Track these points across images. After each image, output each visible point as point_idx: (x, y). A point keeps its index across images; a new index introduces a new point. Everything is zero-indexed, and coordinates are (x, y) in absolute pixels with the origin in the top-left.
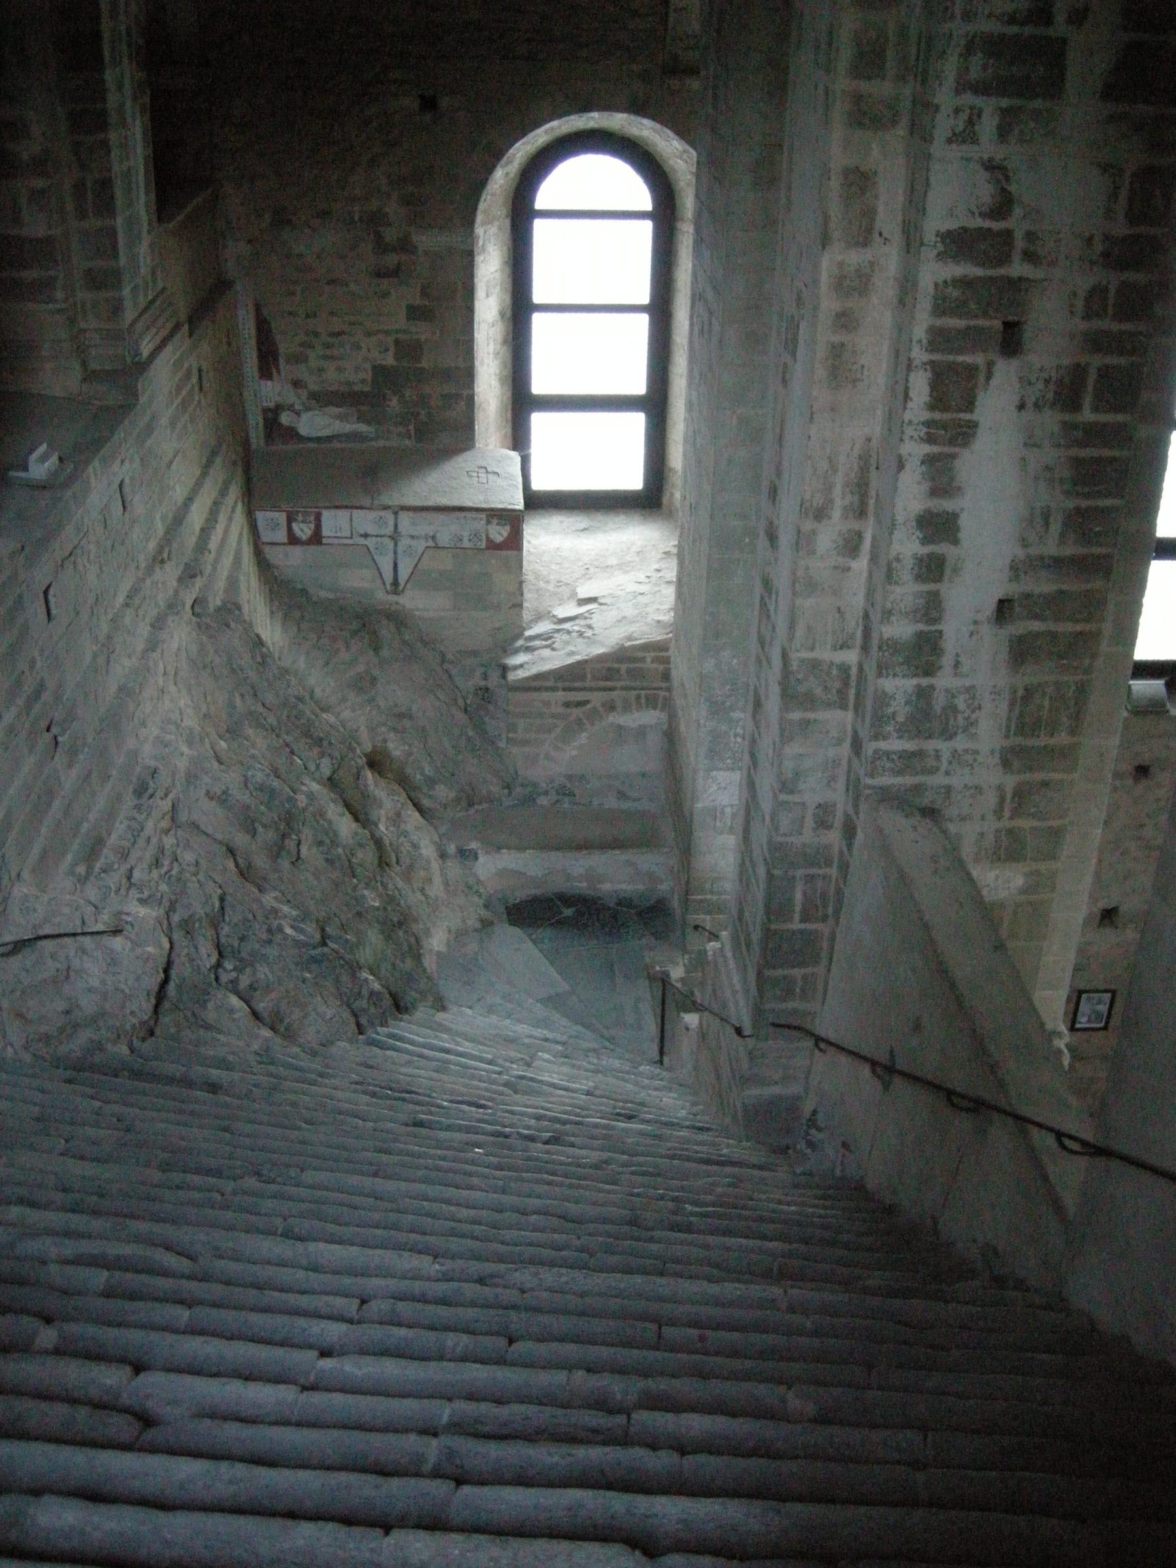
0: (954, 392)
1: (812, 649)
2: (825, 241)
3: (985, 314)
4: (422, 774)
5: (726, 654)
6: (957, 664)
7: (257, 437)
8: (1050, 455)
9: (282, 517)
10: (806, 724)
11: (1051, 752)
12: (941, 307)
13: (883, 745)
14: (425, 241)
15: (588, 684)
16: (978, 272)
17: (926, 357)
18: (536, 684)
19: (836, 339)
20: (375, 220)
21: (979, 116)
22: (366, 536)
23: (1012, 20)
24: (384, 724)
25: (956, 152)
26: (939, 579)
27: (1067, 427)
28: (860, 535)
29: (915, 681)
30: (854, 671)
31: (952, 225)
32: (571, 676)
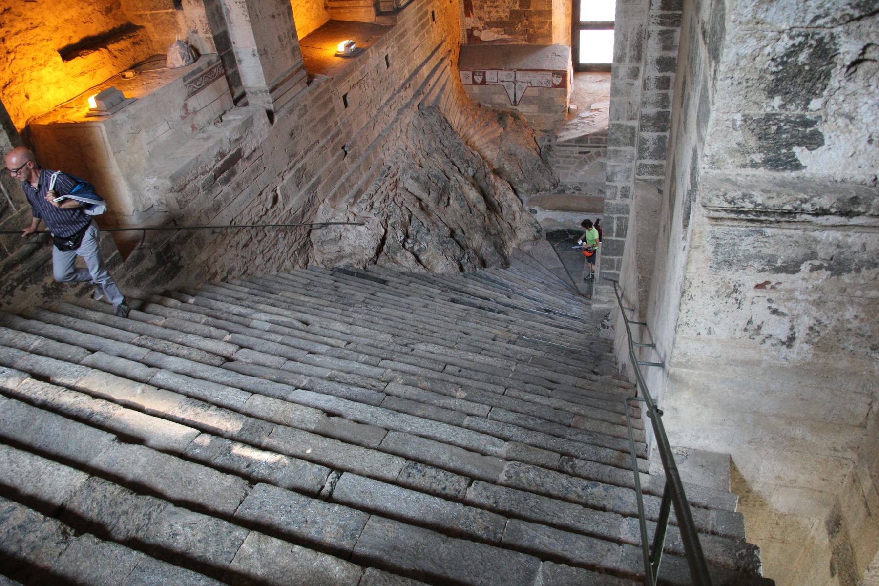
1: (618, 119)
9: (470, 74)
10: (616, 152)
15: (589, 144)
22: (503, 81)
26: (667, 88)
28: (638, 69)
32: (582, 140)
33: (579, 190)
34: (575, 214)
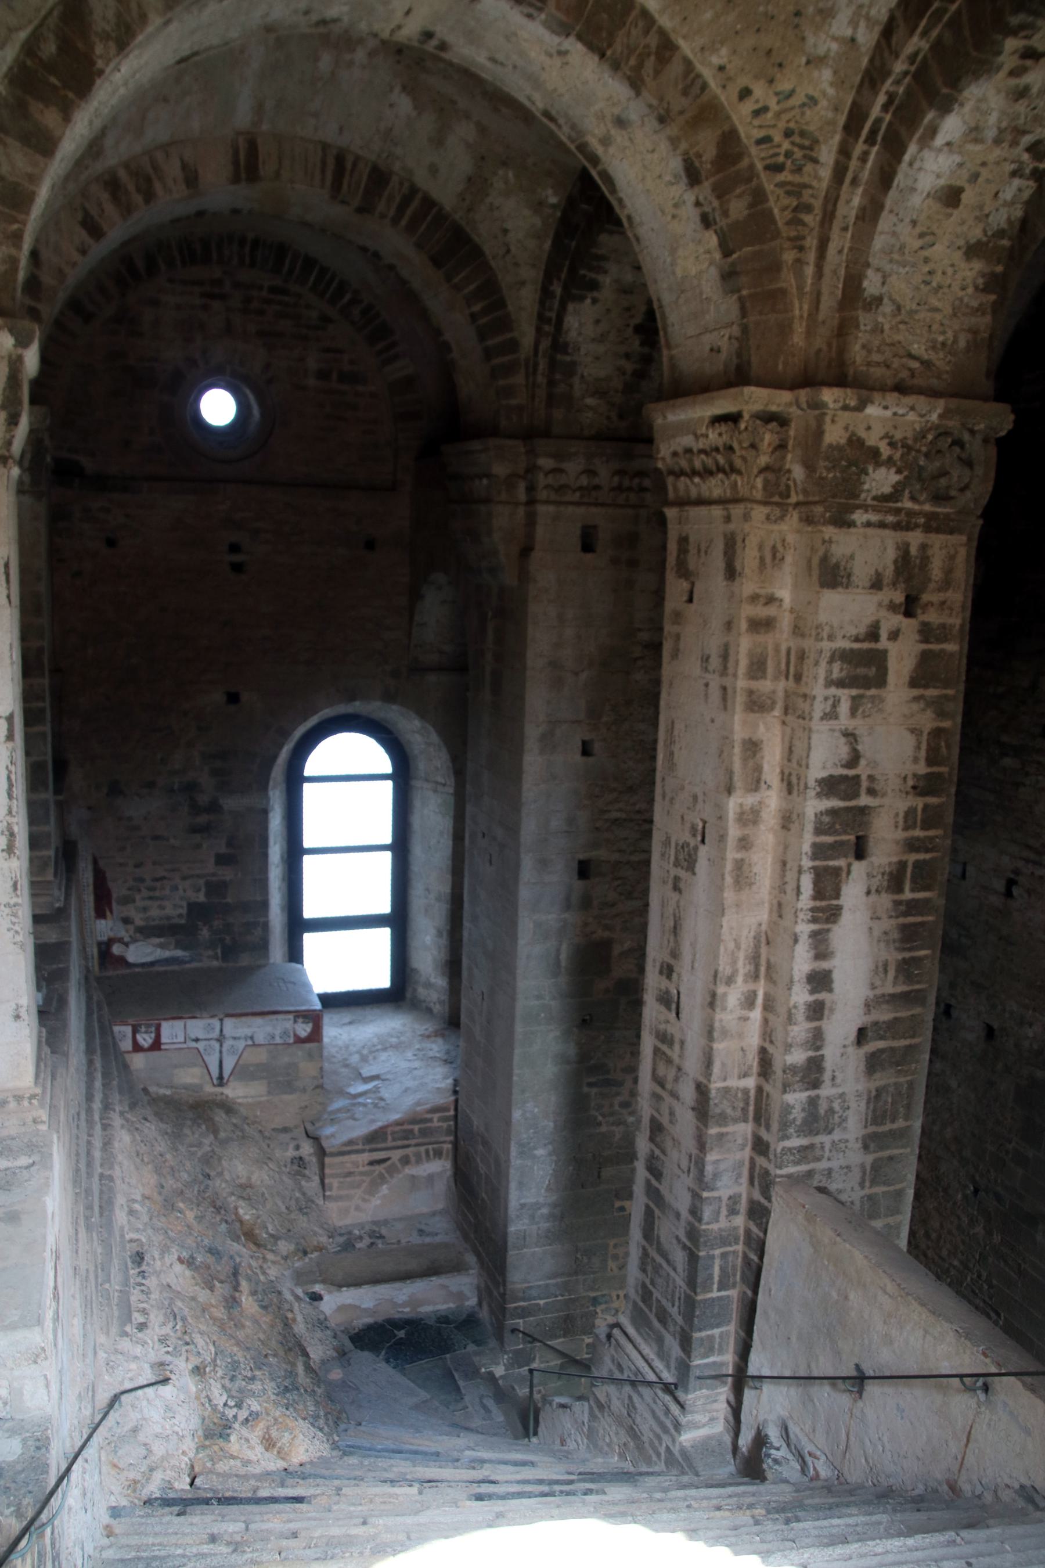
0: (828, 885)
1: (725, 1079)
2: (729, 790)
3: (845, 832)
4: (267, 1233)
5: (530, 1105)
6: (833, 1078)
9: (128, 1030)
10: (721, 1135)
11: (892, 1133)
12: (818, 831)
14: (230, 803)
15: (390, 1143)
16: (841, 804)
17: (810, 864)
18: (349, 1148)
19: (739, 856)
20: (191, 788)
22: (197, 1040)
23: (857, 640)
24: (233, 1194)
25: (825, 726)
26: (820, 1018)
27: (898, 903)
28: (754, 993)
29: (807, 1094)
30: (752, 1093)
31: (824, 774)
33: (382, 1237)
34: (397, 1285)
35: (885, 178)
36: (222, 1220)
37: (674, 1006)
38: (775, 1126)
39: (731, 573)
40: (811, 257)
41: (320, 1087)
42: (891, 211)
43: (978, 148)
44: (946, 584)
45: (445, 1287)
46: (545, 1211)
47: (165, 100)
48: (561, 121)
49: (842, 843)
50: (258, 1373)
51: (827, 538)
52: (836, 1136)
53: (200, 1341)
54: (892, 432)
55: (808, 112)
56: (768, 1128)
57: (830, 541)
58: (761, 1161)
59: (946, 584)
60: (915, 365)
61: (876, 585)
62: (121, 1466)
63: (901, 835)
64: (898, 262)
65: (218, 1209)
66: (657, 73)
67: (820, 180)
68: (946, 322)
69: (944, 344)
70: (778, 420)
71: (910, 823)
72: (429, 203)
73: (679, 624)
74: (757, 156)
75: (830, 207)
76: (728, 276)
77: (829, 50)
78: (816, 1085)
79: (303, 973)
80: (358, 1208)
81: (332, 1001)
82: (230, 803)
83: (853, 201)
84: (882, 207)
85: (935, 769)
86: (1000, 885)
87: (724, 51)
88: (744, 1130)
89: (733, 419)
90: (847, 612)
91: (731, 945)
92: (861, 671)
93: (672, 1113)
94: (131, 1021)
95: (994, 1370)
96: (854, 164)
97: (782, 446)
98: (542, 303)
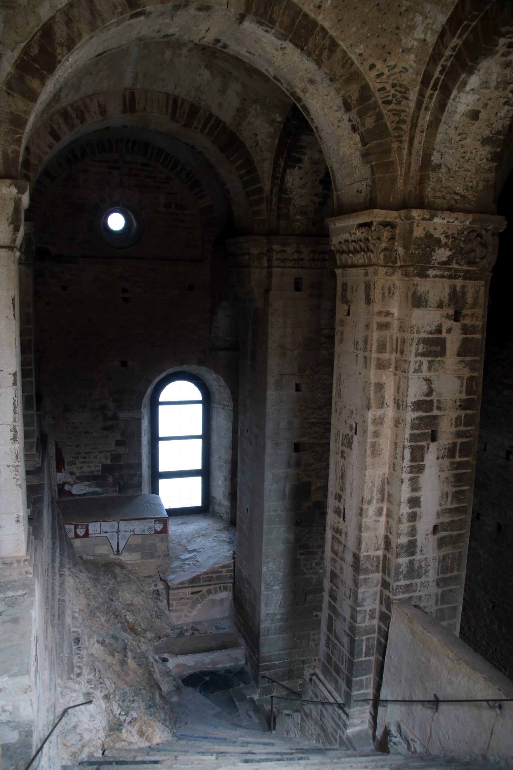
0: (418, 455)
1: (368, 551)
2: (369, 408)
3: (426, 428)
4: (141, 628)
5: (271, 564)
6: (421, 551)
7: (56, 495)
8: (447, 474)
9: (73, 527)
10: (366, 579)
11: (451, 578)
12: (413, 428)
13: (399, 583)
14: (123, 415)
15: (201, 583)
16: (424, 414)
17: (409, 444)
19: (373, 440)
21: (422, 363)
22: (106, 532)
24: (124, 609)
25: (415, 376)
26: (415, 521)
27: (452, 463)
28: (382, 508)
30: (381, 558)
31: (415, 399)
33: (197, 630)
34: (205, 654)
35: (442, 107)
36: (118, 621)
37: (342, 515)
38: (393, 574)
39: (368, 301)
40: (406, 145)
41: (168, 555)
42: (445, 123)
43: (487, 91)
44: (475, 305)
45: (229, 655)
46: (278, 617)
47: (91, 74)
48: (283, 81)
49: (424, 434)
50: (136, 698)
51: (415, 283)
52: (423, 579)
53: (107, 682)
54: (447, 231)
55: (403, 75)
56: (389, 575)
57: (417, 285)
58: (386, 592)
59: (475, 305)
60: (458, 197)
61: (440, 306)
62: (68, 745)
63: (454, 429)
64: (448, 148)
65: (116, 616)
66: (329, 57)
67: (409, 108)
68: (473, 176)
69: (472, 187)
70: (391, 225)
71: (458, 423)
72: (218, 121)
73: (343, 326)
74: (378, 97)
75: (415, 122)
76: (365, 155)
77: (413, 45)
78: (413, 554)
79: (159, 499)
80: (186, 616)
81: (173, 513)
82: (123, 415)
83: (426, 118)
84: (440, 120)
85: (471, 397)
86: (503, 454)
87: (362, 47)
88: (377, 576)
89: (368, 225)
90: (426, 319)
91: (370, 485)
92: (433, 348)
93: (341, 568)
94: (74, 523)
95: (504, 698)
96: (426, 100)
97: (392, 238)
98: (274, 169)
